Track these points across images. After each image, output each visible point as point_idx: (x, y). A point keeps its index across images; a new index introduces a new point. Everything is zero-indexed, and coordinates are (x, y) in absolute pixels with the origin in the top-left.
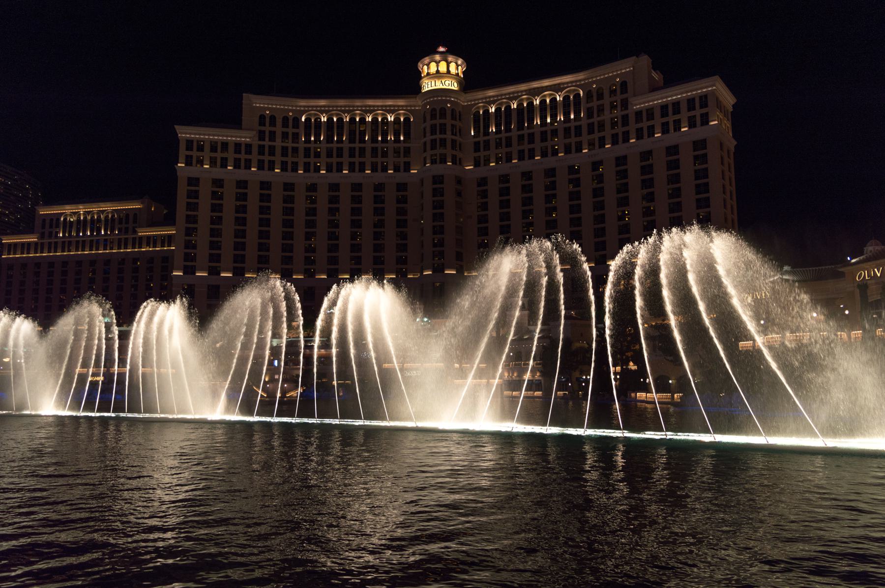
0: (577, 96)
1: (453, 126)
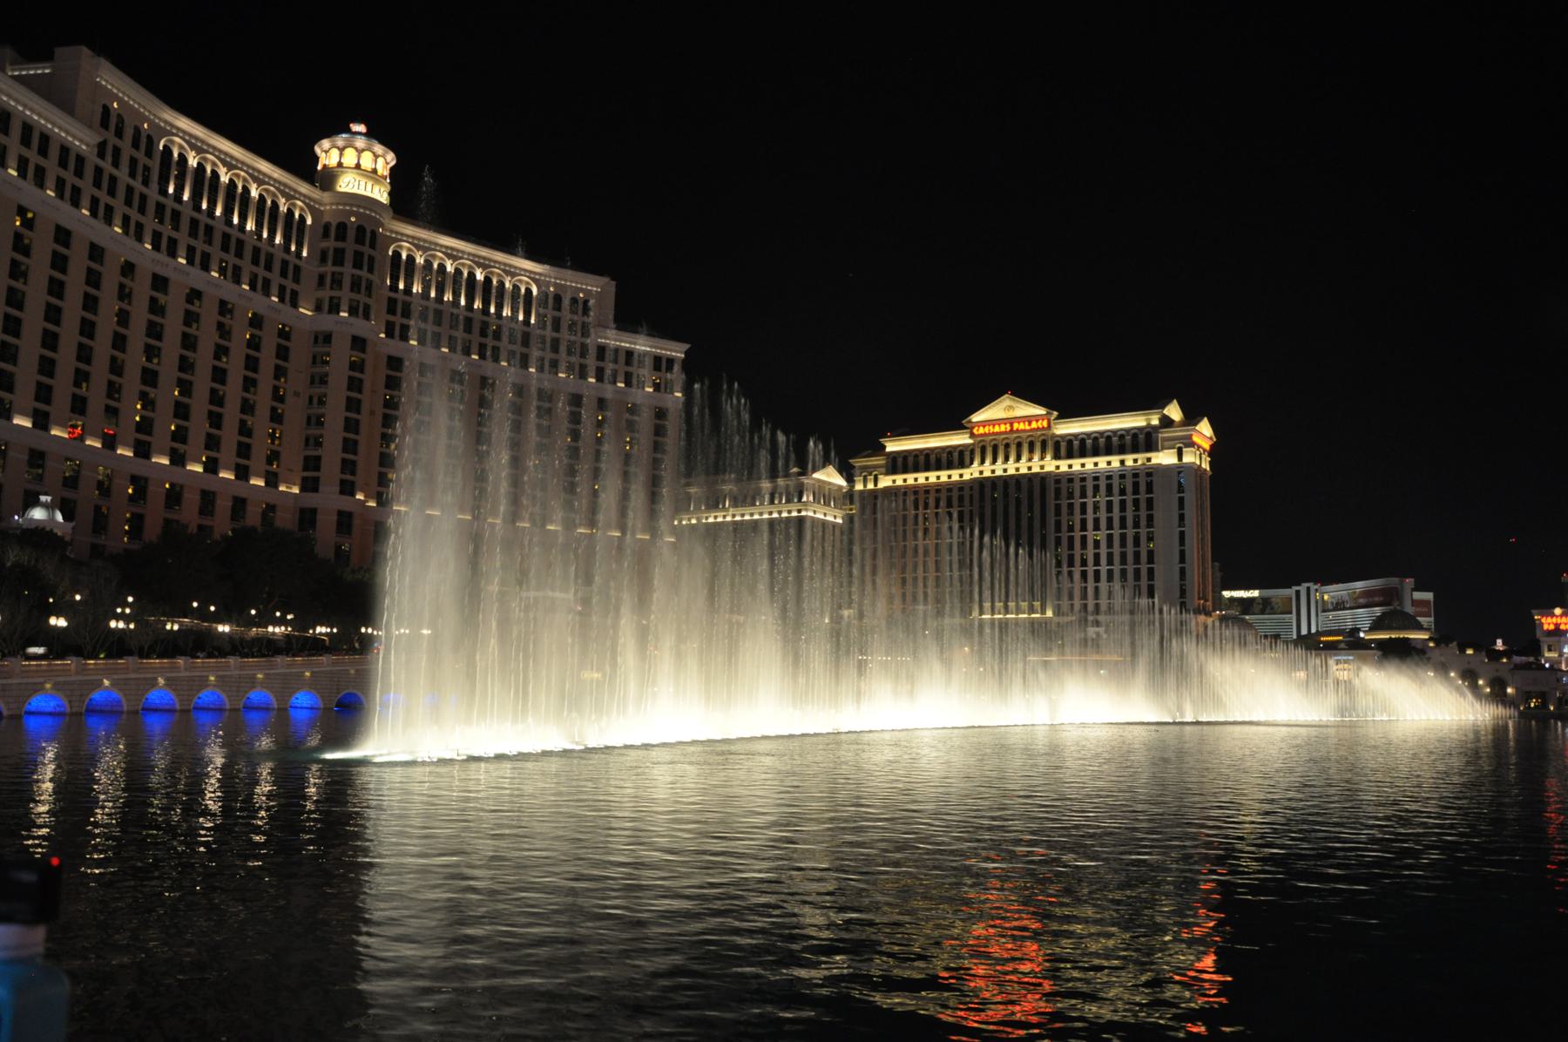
0: (529, 291)
1: (356, 253)
